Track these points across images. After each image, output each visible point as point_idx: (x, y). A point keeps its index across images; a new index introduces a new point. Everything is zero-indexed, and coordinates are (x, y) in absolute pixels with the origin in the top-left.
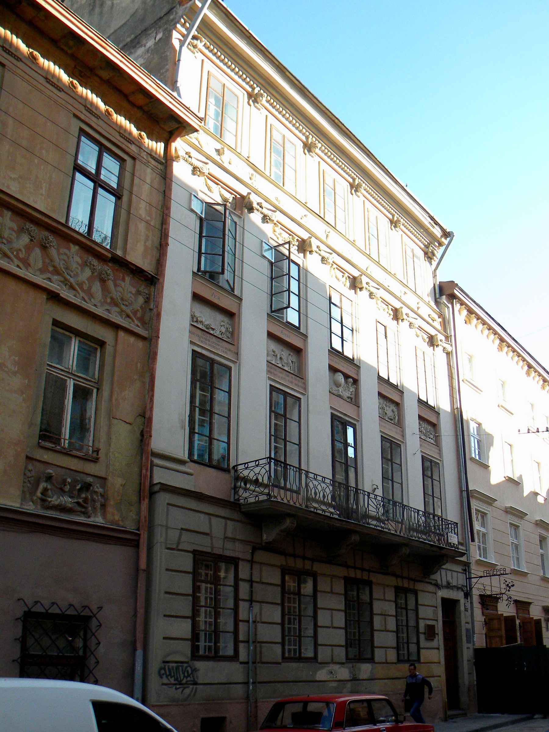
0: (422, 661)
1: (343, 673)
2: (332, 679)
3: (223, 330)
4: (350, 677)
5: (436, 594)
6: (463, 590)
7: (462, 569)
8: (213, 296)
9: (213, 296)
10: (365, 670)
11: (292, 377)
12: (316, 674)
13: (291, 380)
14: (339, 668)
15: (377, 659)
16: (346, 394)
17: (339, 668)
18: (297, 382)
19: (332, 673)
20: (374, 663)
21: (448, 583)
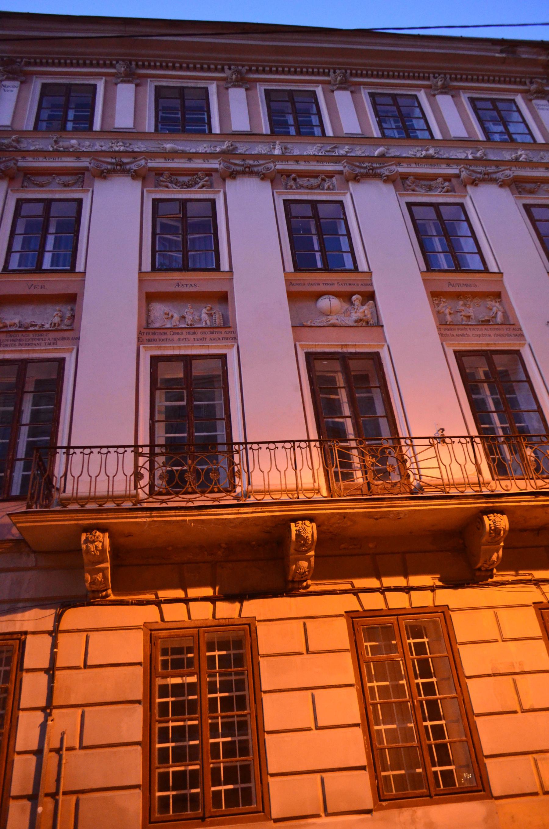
3: (57, 320)
8: (33, 287)
9: (33, 287)
11: (202, 333)
13: (199, 336)
18: (213, 336)
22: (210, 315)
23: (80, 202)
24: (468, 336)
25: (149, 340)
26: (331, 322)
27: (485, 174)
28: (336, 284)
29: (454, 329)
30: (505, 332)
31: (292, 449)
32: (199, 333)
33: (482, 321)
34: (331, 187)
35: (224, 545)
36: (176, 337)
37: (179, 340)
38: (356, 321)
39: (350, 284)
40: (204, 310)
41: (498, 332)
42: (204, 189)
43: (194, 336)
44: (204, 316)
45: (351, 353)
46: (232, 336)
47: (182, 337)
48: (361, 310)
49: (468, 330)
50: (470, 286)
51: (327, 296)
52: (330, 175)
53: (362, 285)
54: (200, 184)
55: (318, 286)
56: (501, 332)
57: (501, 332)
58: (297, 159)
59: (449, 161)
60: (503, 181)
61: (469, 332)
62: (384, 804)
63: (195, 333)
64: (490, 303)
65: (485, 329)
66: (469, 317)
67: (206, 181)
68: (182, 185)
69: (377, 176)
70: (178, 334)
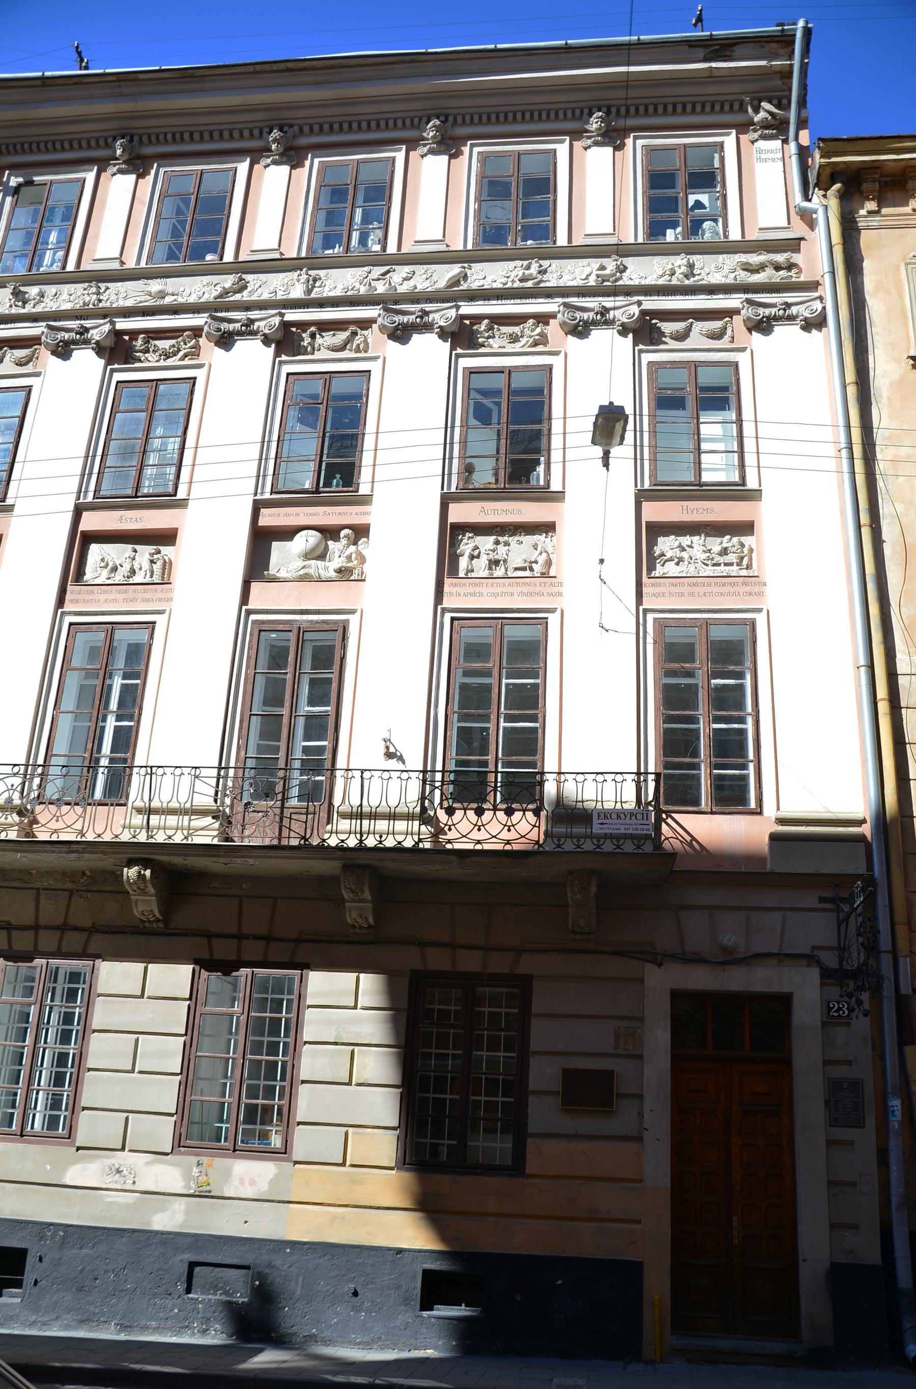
0: (530, 1168)
1: (169, 1175)
2: (119, 1187)
4: (187, 1186)
5: (641, 981)
6: (819, 963)
7: (822, 900)
10: (249, 1175)
11: (134, 591)
12: (64, 1171)
13: (131, 595)
14: (148, 1164)
15: (298, 1152)
16: (329, 568)
17: (148, 1164)
19: (118, 1171)
20: (288, 1160)
21: (725, 950)
22: (152, 562)
23: (29, 389)
24: (481, 594)
25: (71, 601)
26: (302, 572)
27: (597, 313)
28: (321, 514)
29: (464, 585)
30: (538, 589)
31: (148, 777)
32: (131, 591)
33: (516, 569)
34: (361, 346)
35: (88, 873)
36: (103, 597)
37: (106, 601)
38: (339, 571)
39: (340, 514)
40: (147, 556)
41: (525, 589)
42: (187, 362)
43: (123, 596)
44: (146, 565)
45: (311, 621)
46: (169, 595)
47: (110, 596)
48: (347, 553)
49: (485, 585)
50: (512, 512)
51: (305, 532)
52: (365, 324)
53: (356, 514)
54: (181, 354)
55: (298, 517)
56: (532, 589)
57: (532, 589)
58: (322, 303)
59: (550, 293)
60: (623, 325)
61: (484, 590)
62: (182, 1149)
63: (126, 592)
64: (540, 538)
65: (509, 584)
66: (496, 563)
67: (191, 348)
68: (160, 355)
69: (426, 327)
70: (106, 592)
